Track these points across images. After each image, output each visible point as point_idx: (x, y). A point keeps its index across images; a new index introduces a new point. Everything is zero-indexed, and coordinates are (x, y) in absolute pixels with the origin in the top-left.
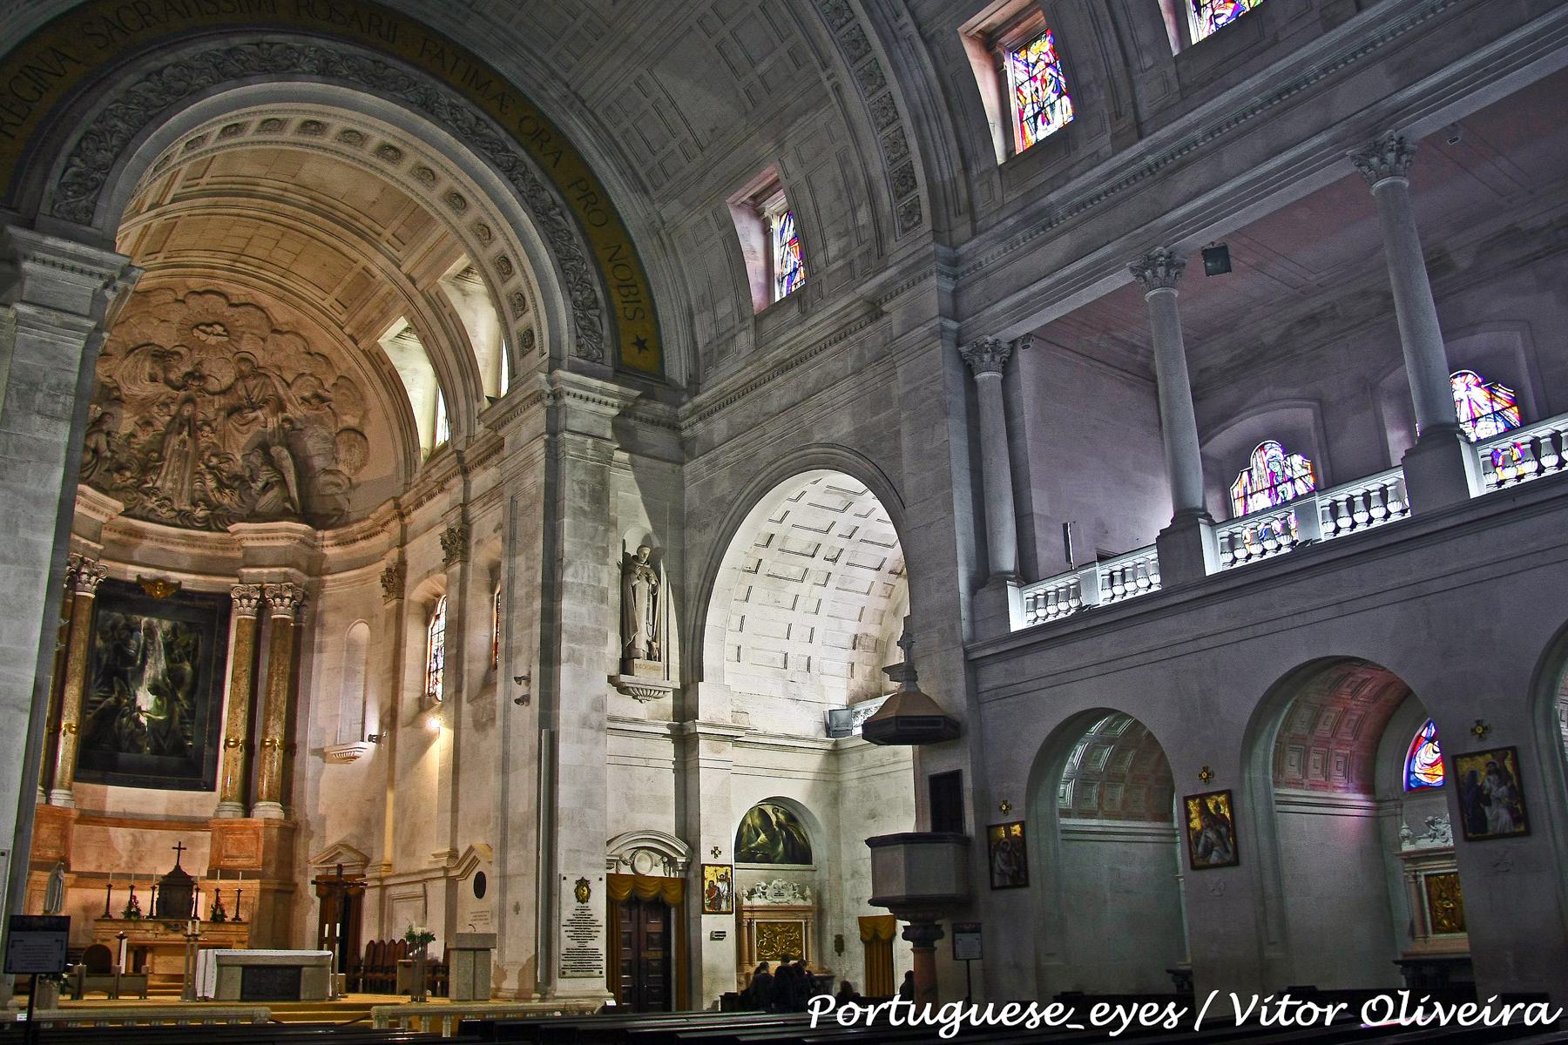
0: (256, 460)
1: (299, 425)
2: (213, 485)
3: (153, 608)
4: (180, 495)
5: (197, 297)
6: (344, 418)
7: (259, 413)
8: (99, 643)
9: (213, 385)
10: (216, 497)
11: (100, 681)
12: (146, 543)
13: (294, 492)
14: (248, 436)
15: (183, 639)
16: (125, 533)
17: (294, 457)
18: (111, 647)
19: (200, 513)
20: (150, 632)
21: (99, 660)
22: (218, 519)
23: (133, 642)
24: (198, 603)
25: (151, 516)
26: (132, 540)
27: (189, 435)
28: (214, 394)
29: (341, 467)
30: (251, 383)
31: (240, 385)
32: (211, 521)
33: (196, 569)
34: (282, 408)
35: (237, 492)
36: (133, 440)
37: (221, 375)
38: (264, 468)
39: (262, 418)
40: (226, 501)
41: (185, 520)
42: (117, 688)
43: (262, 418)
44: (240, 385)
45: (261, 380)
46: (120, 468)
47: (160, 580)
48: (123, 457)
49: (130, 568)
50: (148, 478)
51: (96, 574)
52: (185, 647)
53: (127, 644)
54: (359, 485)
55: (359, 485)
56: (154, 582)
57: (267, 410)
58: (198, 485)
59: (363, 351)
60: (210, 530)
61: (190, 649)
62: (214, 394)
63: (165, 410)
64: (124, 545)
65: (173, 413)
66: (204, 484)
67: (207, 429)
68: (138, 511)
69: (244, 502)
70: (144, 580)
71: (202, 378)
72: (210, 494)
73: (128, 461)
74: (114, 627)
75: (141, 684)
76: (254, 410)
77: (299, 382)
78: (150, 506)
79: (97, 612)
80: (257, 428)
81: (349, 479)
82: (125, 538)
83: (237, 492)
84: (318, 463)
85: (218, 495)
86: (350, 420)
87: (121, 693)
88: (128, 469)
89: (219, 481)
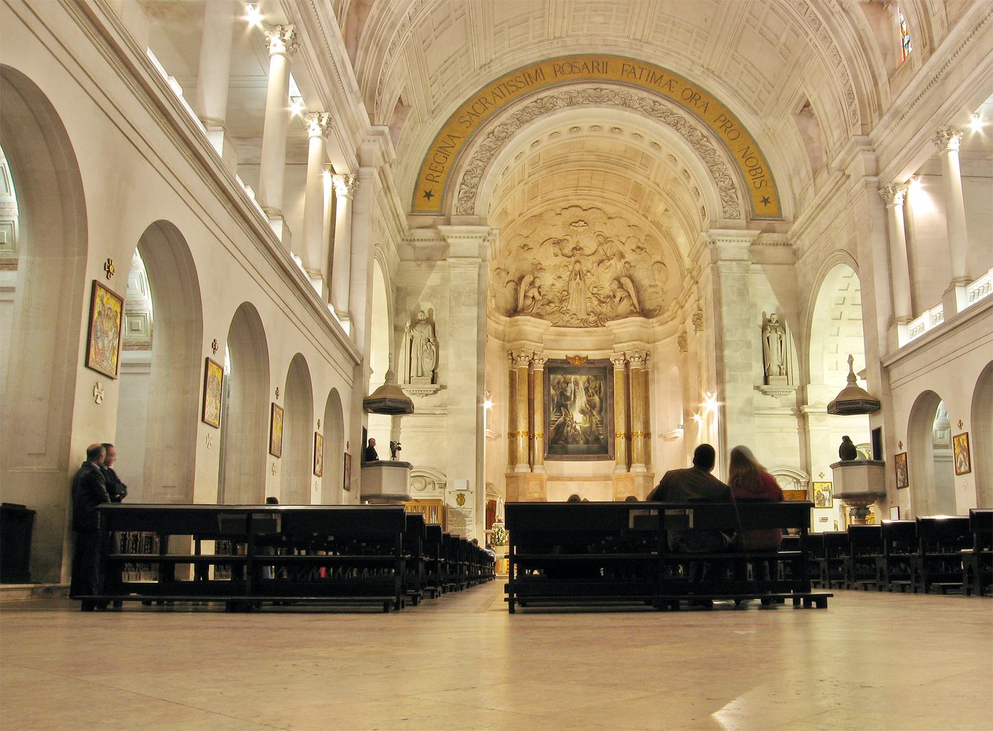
0: (615, 285)
1: (633, 264)
2: (596, 302)
3: (576, 370)
4: (581, 311)
5: (566, 210)
6: (654, 256)
7: (611, 261)
8: (552, 392)
9: (588, 252)
10: (598, 309)
11: (555, 410)
12: (568, 338)
13: (635, 302)
14: (610, 274)
15: (593, 385)
16: (557, 335)
17: (633, 281)
18: (558, 393)
19: (592, 318)
20: (576, 383)
21: (553, 400)
22: (601, 320)
23: (569, 389)
24: (597, 365)
25: (568, 325)
26: (560, 337)
27: (580, 279)
28: (589, 256)
29: (657, 283)
30: (605, 247)
31: (600, 249)
32: (598, 322)
33: (594, 348)
34: (622, 256)
35: (609, 305)
36: (553, 287)
37: (590, 244)
38: (618, 290)
39: (614, 264)
40: (604, 310)
41: (584, 324)
42: (564, 413)
43: (614, 264)
44: (600, 249)
45: (609, 244)
46: (550, 302)
47: (577, 356)
48: (550, 297)
49: (561, 352)
50: (563, 305)
51: (542, 359)
52: (594, 389)
53: (566, 391)
54: (667, 291)
55: (667, 291)
56: (575, 358)
57: (615, 259)
58: (589, 304)
59: (651, 221)
60: (598, 326)
61: (597, 389)
62: (589, 256)
63: (566, 268)
64: (557, 341)
65: (571, 269)
66: (592, 303)
67: (588, 274)
68: (560, 323)
69: (613, 309)
70: (571, 358)
71: (580, 249)
72: (596, 308)
73: (553, 298)
74: (558, 383)
75: (575, 410)
76: (609, 260)
77: (629, 241)
78: (566, 319)
79: (549, 378)
80: (612, 269)
81: (662, 289)
82: (557, 337)
83: (609, 305)
84: (646, 282)
85: (600, 307)
86: (658, 258)
87: (566, 415)
88: (553, 302)
89: (599, 300)
